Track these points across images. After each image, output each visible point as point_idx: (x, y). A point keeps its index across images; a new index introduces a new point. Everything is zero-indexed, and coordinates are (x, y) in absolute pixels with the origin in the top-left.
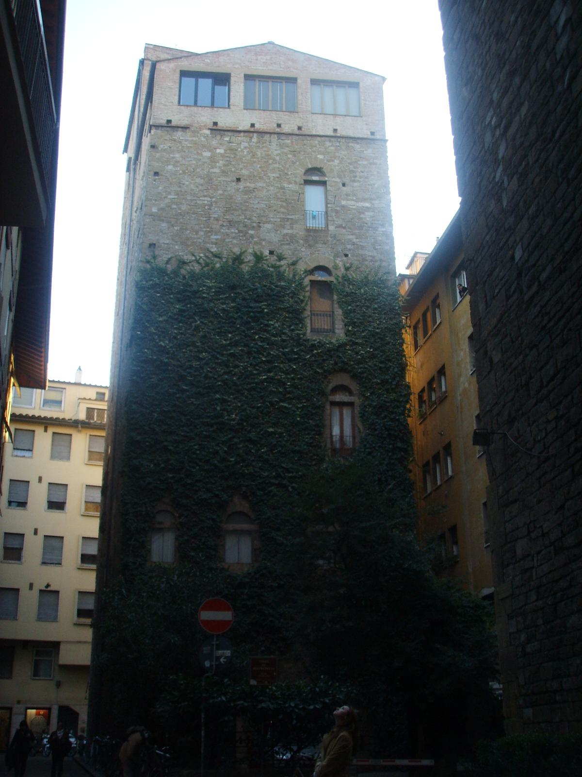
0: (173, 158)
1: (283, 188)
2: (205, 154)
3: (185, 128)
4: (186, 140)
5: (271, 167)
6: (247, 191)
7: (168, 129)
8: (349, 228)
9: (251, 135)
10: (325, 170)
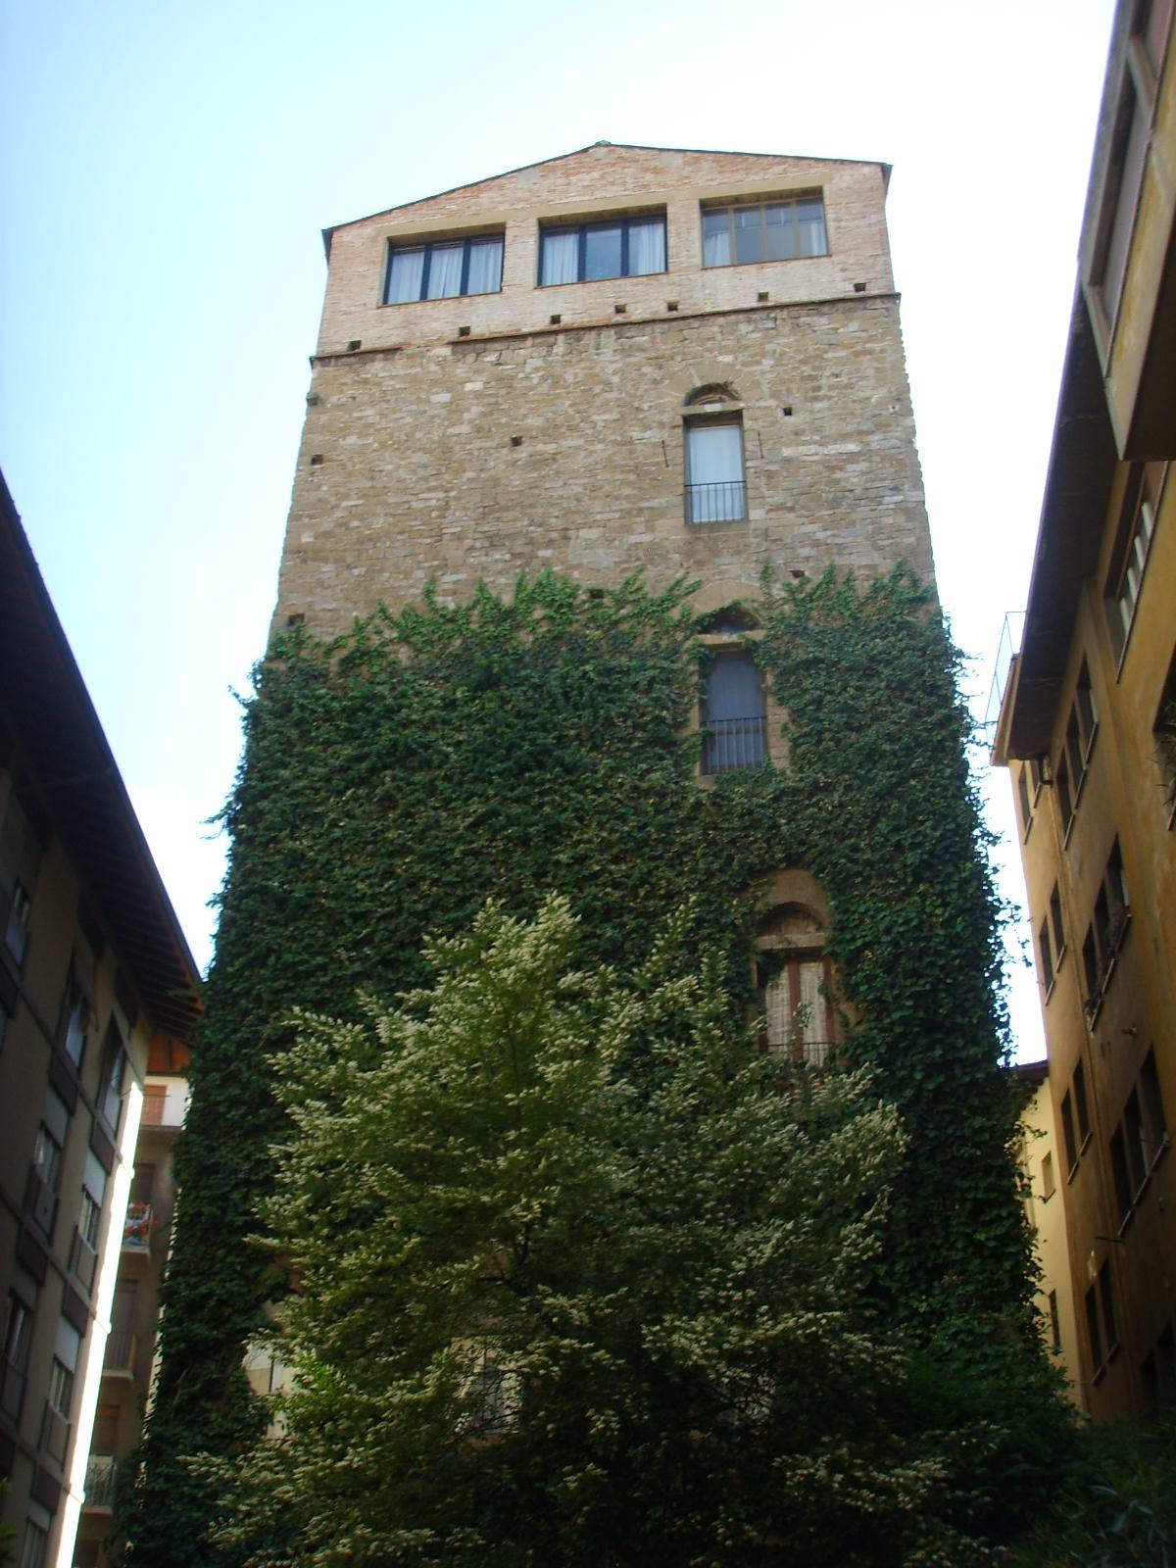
0: (360, 418)
1: (630, 442)
2: (435, 398)
3: (391, 351)
4: (393, 377)
5: (598, 402)
6: (538, 462)
7: (352, 360)
8: (803, 508)
9: (551, 339)
10: (737, 386)
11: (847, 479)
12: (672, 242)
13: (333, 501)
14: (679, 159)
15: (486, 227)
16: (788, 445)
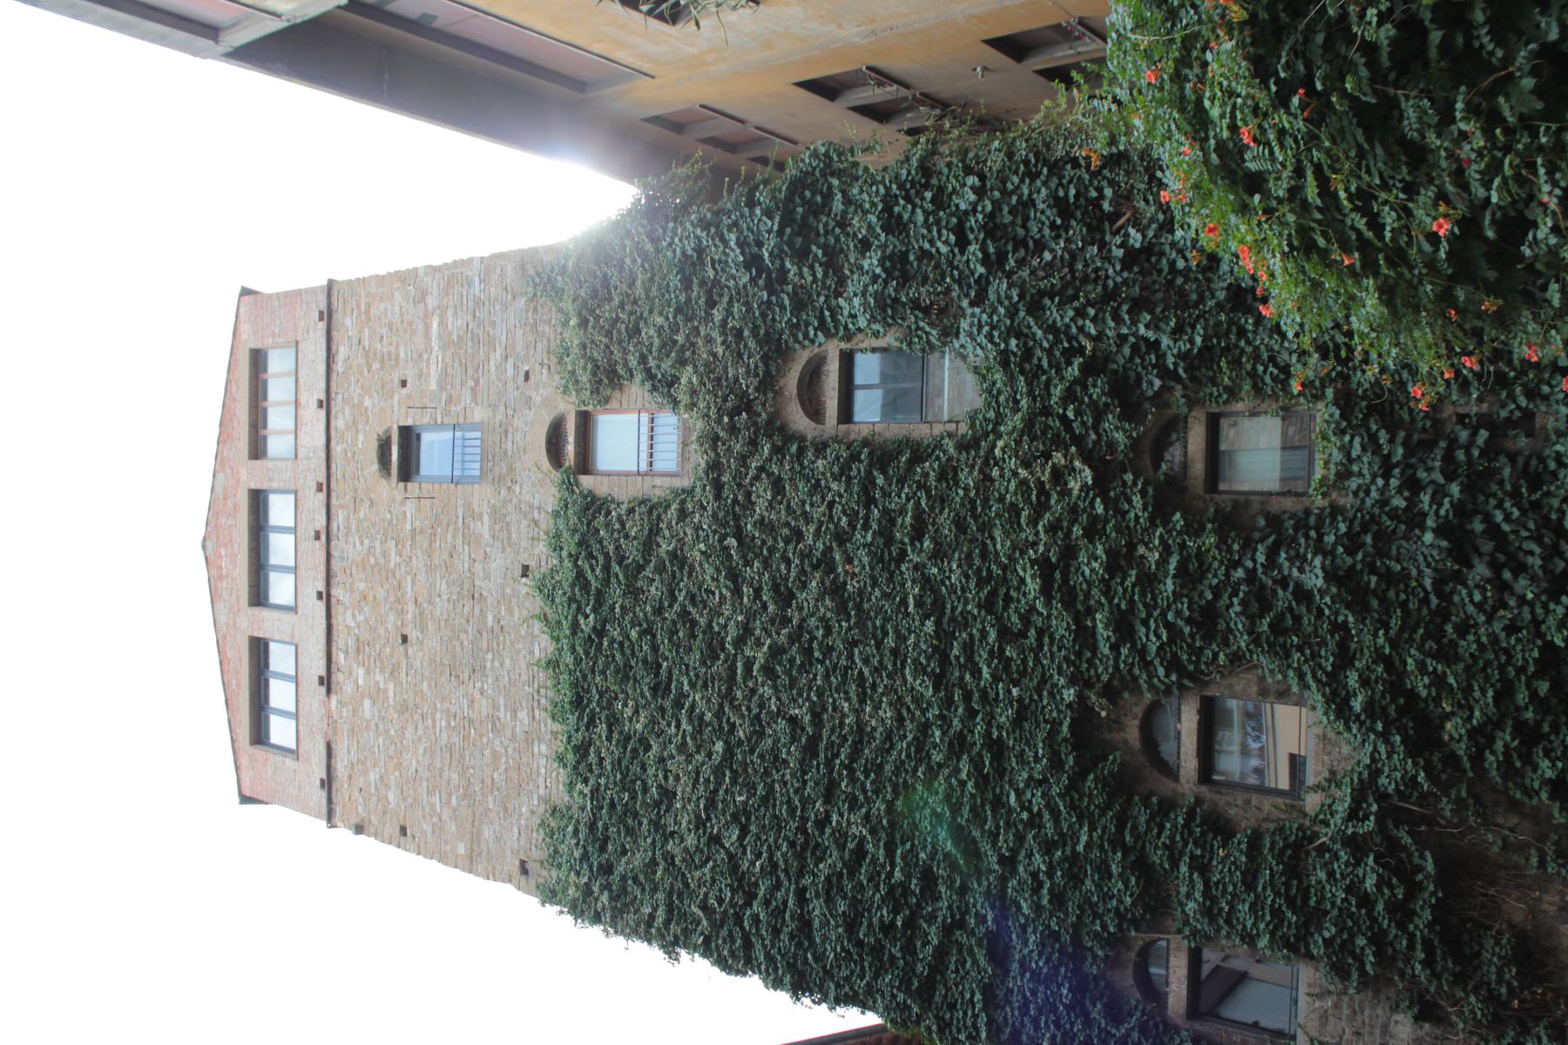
1: (414, 530)
5: (382, 560)
10: (381, 431)
14: (220, 476)
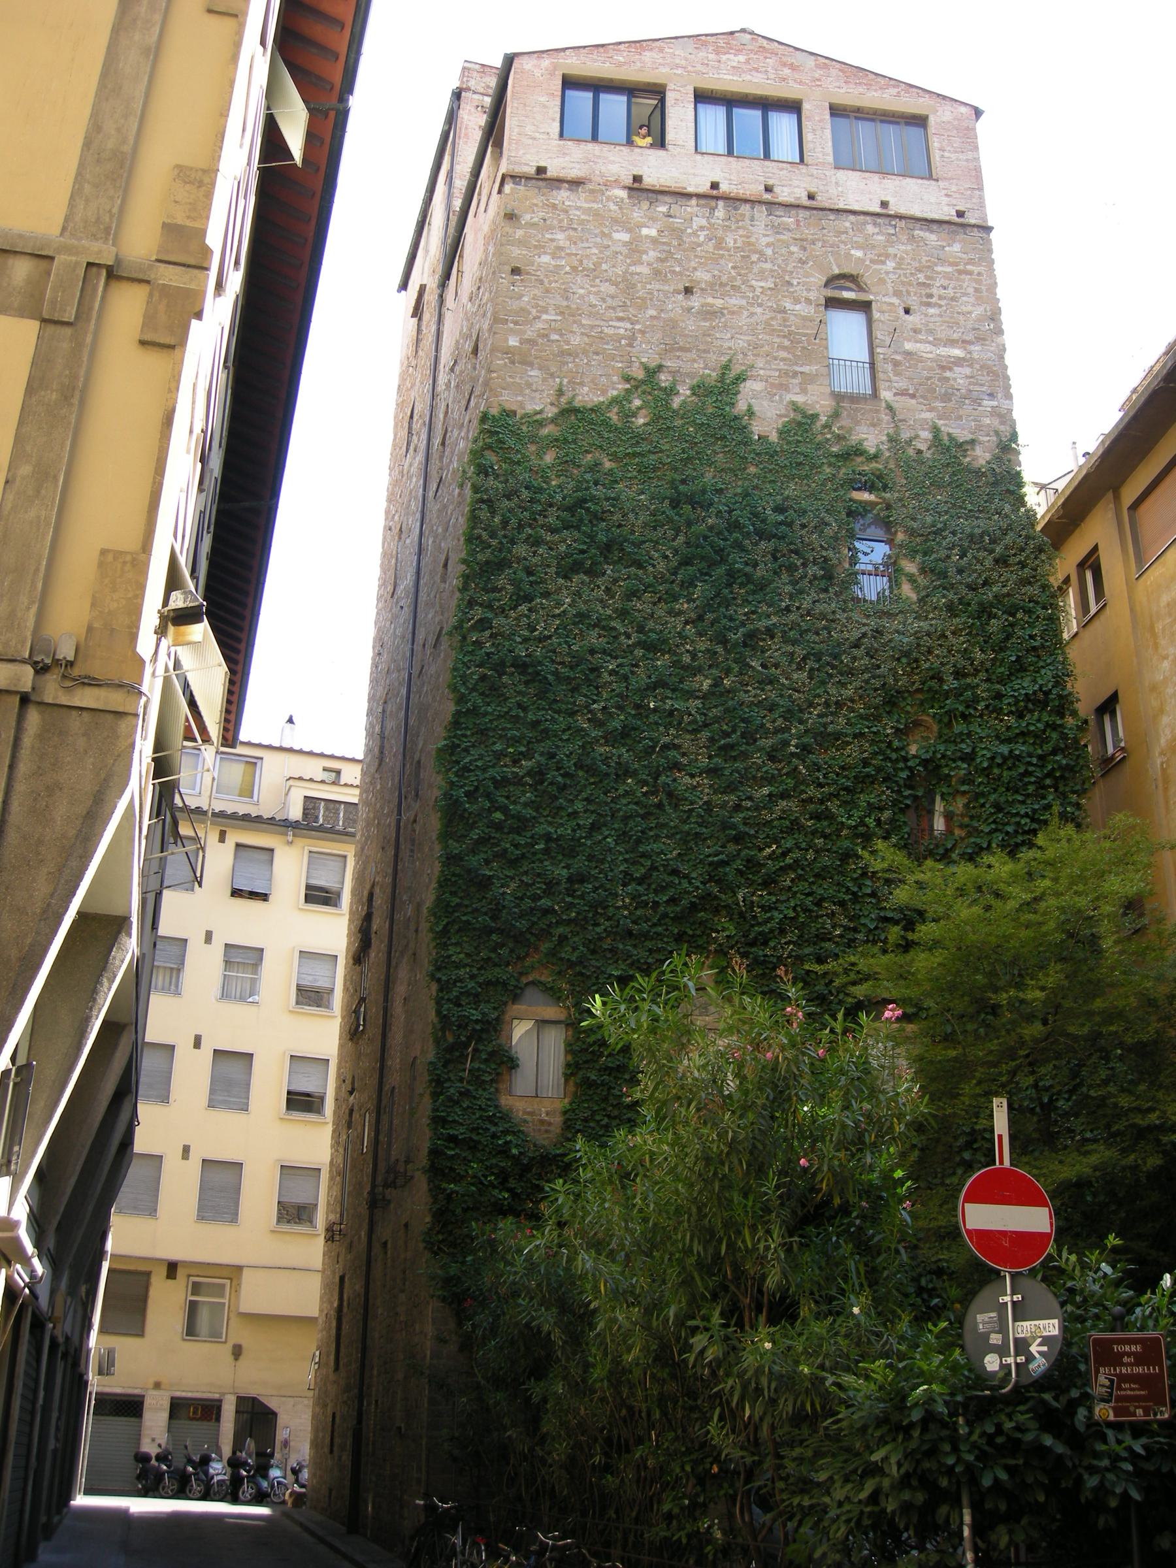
0: (552, 240)
1: (784, 311)
2: (616, 236)
3: (576, 184)
4: (578, 208)
6: (709, 313)
7: (540, 183)
8: (922, 397)
9: (713, 203)
11: (955, 379)
12: (808, 137)
13: (534, 312)
14: (811, 62)
15: (649, 84)
16: (909, 341)
